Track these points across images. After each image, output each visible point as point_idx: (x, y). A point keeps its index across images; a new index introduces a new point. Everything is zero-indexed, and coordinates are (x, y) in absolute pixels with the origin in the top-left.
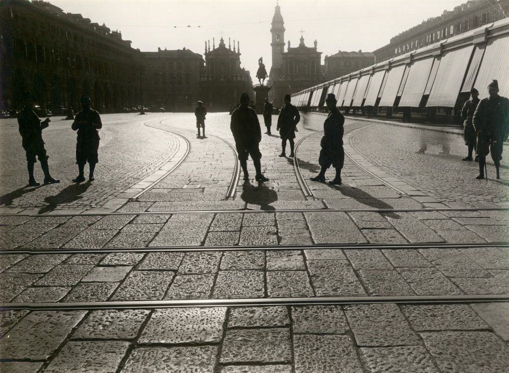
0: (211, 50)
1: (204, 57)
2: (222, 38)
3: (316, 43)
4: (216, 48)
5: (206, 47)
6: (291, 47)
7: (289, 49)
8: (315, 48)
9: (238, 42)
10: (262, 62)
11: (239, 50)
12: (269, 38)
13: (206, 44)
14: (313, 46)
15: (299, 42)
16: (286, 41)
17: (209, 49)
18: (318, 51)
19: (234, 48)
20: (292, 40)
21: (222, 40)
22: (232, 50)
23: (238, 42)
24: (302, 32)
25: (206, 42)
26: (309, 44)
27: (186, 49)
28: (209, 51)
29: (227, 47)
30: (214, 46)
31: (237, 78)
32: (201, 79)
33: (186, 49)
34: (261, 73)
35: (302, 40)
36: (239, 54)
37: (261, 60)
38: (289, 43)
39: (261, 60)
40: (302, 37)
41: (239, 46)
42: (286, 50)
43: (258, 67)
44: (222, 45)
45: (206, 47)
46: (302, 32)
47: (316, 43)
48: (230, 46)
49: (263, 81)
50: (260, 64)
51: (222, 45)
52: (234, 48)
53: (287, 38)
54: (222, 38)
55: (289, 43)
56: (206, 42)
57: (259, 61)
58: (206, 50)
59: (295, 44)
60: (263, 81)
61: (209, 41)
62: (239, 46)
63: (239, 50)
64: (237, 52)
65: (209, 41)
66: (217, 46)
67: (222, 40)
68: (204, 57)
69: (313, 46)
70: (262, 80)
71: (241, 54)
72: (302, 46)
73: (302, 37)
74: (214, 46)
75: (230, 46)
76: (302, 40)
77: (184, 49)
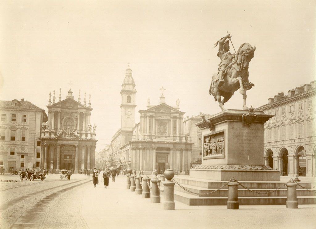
0: (57, 101)
1: (47, 110)
4: (62, 100)
9: (90, 96)
11: (90, 104)
12: (120, 99)
13: (50, 95)
17: (54, 100)
18: (181, 110)
22: (82, 103)
24: (163, 89)
26: (171, 103)
27: (25, 101)
29: (76, 99)
30: (60, 98)
31: (86, 136)
32: (41, 135)
33: (25, 101)
36: (90, 109)
45: (50, 99)
46: (163, 89)
58: (50, 101)
59: (156, 102)
61: (54, 92)
63: (90, 104)
65: (54, 92)
66: (63, 98)
67: (70, 92)
68: (47, 110)
71: (91, 109)
74: (60, 98)
77: (23, 100)
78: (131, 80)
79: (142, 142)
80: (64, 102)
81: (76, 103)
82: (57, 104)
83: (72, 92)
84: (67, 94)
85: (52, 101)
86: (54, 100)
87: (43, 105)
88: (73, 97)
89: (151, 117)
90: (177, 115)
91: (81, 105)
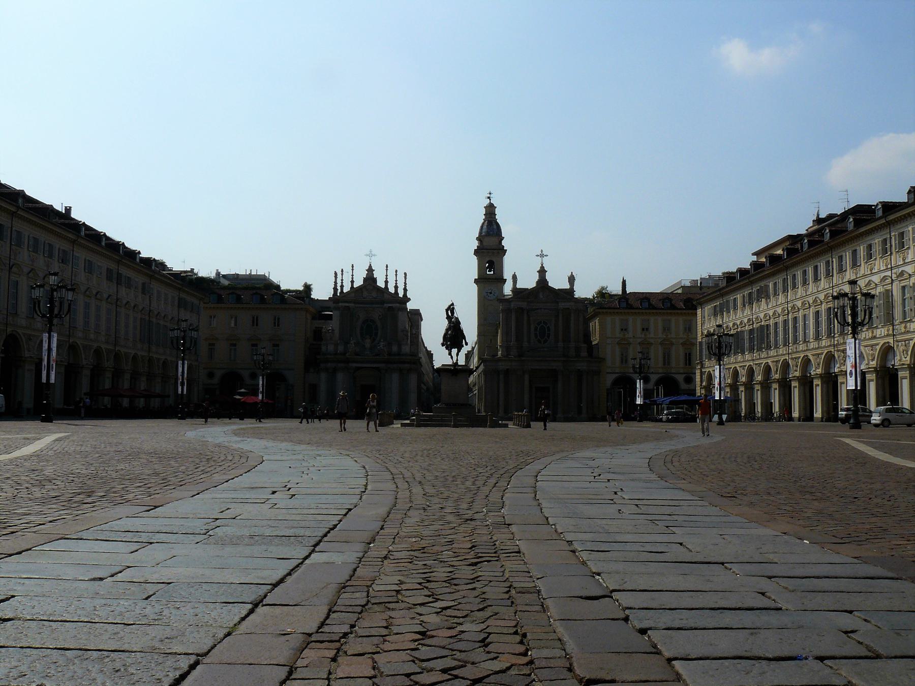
2: (370, 267)
3: (572, 279)
5: (336, 283)
6: (518, 286)
7: (515, 290)
8: (571, 292)
9: (405, 274)
10: (453, 313)
11: (405, 290)
14: (567, 286)
15: (536, 277)
16: (507, 275)
17: (342, 286)
19: (396, 287)
20: (519, 270)
21: (370, 270)
22: (392, 290)
23: (405, 274)
24: (542, 256)
25: (336, 274)
26: (557, 282)
29: (381, 284)
30: (352, 282)
34: (454, 337)
35: (542, 272)
36: (406, 299)
37: (451, 309)
38: (515, 278)
39: (451, 309)
40: (542, 267)
41: (405, 284)
42: (508, 289)
43: (446, 323)
44: (370, 279)
45: (336, 283)
46: (542, 256)
47: (572, 279)
48: (386, 282)
49: (457, 355)
50: (448, 318)
51: (370, 279)
52: (396, 287)
53: (509, 266)
54: (370, 267)
55: (515, 278)
56: (336, 274)
57: (447, 311)
58: (335, 289)
59: (528, 282)
60: (457, 355)
62: (405, 284)
63: (405, 290)
64: (401, 294)
66: (359, 282)
67: (370, 270)
69: (567, 286)
70: (454, 351)
71: (409, 299)
73: (542, 267)
74: (352, 282)
75: (386, 282)
76: (542, 272)
78: (495, 227)
85: (339, 288)
87: (322, 292)
88: (375, 280)
89: (520, 311)
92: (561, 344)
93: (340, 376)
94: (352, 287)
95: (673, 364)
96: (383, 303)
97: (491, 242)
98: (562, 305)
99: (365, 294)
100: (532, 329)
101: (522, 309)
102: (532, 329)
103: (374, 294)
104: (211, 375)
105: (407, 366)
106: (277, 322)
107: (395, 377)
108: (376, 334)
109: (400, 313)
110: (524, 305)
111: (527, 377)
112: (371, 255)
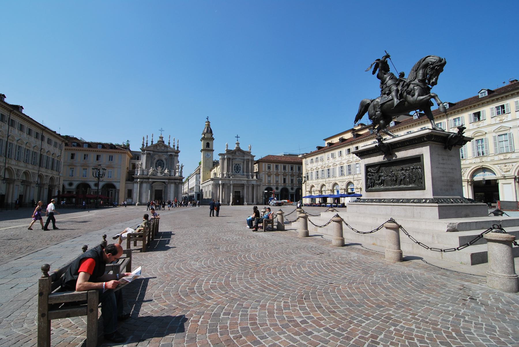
0: (149, 144)
11: (178, 147)
17: (147, 144)
19: (174, 146)
22: (172, 146)
26: (244, 148)
28: (147, 145)
29: (166, 143)
30: (152, 142)
35: (238, 144)
36: (178, 152)
44: (161, 142)
46: (237, 137)
48: (169, 143)
51: (161, 142)
52: (174, 146)
58: (143, 145)
59: (233, 147)
63: (178, 147)
64: (176, 149)
69: (248, 150)
72: (238, 149)
74: (152, 142)
75: (169, 143)
79: (221, 179)
80: (156, 145)
81: (166, 146)
82: (150, 147)
83: (162, 137)
84: (159, 139)
85: (145, 145)
86: (147, 144)
87: (136, 147)
88: (163, 142)
90: (250, 158)
91: (171, 148)
92: (245, 173)
93: (144, 185)
94: (152, 144)
95: (287, 182)
96: (167, 152)
97: (208, 136)
98: (246, 158)
99: (158, 148)
100: (233, 166)
101: (230, 158)
102: (233, 166)
103: (163, 148)
104: (71, 184)
105: (178, 181)
106: (111, 158)
107: (173, 186)
108: (163, 167)
109: (175, 157)
110: (230, 156)
111: (232, 187)
112: (161, 130)
